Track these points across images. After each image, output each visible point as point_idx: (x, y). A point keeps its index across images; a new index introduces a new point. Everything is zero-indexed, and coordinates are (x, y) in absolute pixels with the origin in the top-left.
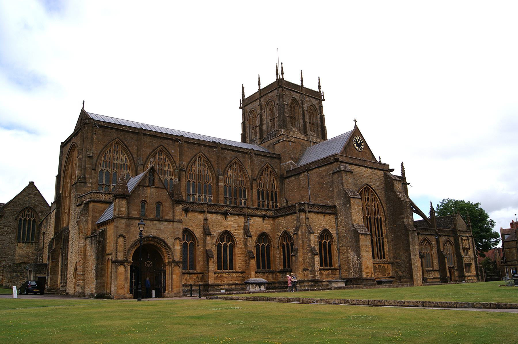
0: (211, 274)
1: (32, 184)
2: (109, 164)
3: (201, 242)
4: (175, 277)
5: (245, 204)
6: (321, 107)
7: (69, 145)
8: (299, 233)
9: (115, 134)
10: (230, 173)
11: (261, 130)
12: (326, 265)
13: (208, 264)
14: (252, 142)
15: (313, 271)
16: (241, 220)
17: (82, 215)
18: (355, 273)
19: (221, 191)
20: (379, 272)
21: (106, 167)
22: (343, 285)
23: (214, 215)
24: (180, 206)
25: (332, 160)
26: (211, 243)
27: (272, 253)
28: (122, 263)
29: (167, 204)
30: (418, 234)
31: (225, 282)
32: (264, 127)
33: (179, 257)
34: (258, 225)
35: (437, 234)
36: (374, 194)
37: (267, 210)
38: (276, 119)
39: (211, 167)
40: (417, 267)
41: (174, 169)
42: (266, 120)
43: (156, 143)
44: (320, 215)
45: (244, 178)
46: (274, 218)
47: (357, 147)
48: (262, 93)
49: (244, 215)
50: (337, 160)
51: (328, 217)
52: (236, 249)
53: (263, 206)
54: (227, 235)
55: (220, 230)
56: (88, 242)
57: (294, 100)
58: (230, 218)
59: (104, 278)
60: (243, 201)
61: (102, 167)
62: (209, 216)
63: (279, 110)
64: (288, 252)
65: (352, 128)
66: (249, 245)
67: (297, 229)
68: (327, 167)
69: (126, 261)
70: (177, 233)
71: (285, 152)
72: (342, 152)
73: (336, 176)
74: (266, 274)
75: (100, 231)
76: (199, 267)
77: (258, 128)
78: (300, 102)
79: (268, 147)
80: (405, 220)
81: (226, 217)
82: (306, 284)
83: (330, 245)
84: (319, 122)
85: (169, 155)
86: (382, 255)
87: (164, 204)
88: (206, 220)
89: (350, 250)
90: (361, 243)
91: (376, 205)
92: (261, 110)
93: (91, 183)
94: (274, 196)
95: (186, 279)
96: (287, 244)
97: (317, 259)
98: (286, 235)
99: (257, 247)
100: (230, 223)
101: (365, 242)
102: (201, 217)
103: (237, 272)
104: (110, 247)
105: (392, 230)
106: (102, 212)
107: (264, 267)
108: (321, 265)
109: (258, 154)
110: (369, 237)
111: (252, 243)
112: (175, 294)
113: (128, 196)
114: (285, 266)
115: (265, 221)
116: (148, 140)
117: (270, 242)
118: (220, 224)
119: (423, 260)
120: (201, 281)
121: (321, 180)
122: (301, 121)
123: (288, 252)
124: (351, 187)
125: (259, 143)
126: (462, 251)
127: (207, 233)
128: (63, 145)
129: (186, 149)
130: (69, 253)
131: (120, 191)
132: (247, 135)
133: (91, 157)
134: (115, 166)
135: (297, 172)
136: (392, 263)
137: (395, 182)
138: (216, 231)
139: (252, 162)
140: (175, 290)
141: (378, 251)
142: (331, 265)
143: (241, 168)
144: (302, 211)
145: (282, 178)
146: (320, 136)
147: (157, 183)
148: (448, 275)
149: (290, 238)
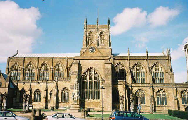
10: (57, 67)
20: (94, 105)
31: (36, 106)
43: (29, 61)
47: (91, 51)
55: (36, 89)
88: (31, 86)
91: (97, 76)
118: (35, 87)
138: (34, 90)
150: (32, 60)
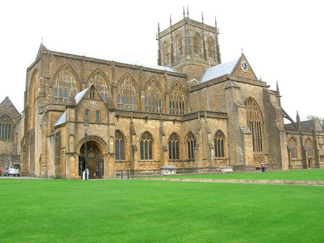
0: (136, 163)
1: (7, 98)
2: (62, 83)
3: (128, 139)
4: (110, 165)
5: (160, 111)
6: (217, 39)
7: (33, 70)
8: (200, 133)
9: (65, 61)
10: (149, 88)
11: (172, 56)
12: (219, 156)
13: (133, 155)
14: (165, 65)
15: (210, 161)
16: (158, 123)
17: (43, 120)
18: (240, 161)
19: (143, 102)
21: (60, 85)
22: (231, 170)
23: (138, 120)
24: (113, 113)
25: (225, 79)
26: (136, 140)
27: (180, 147)
28: (72, 154)
29: (104, 112)
30: (287, 134)
32: (175, 54)
33: (112, 150)
34: (170, 127)
35: (300, 134)
36: (256, 103)
37: (177, 116)
38: (184, 48)
39: (135, 85)
40: (285, 157)
41: (108, 86)
42: (176, 49)
43: (94, 67)
44: (215, 119)
45: (159, 92)
46: (181, 122)
48: (173, 28)
49: (160, 120)
50: (228, 79)
51: (221, 121)
52: (154, 144)
53: (174, 113)
54: (147, 134)
55: (143, 131)
56: (48, 139)
57: (197, 33)
58: (149, 122)
59: (60, 165)
60: (159, 109)
61: (57, 86)
62: (134, 120)
63: (186, 41)
64: (192, 147)
65: (239, 56)
66: (164, 141)
67: (199, 130)
68: (221, 84)
69: (75, 153)
70: (111, 133)
71: (190, 72)
72: (233, 73)
73: (227, 91)
74: (176, 163)
75: (56, 131)
76: (127, 158)
77: (170, 55)
78: (201, 35)
79: (178, 68)
80: (277, 124)
81: (146, 121)
82: (205, 170)
83: (222, 142)
84: (216, 50)
85: (104, 76)
86: (261, 149)
87: (101, 112)
88: (132, 123)
89: (237, 146)
90: (245, 140)
92: (172, 41)
93: (49, 97)
94: (182, 105)
95: (118, 166)
96: (192, 141)
97: (213, 152)
98: (190, 135)
99: (170, 143)
100: (149, 126)
101: (248, 140)
102: (128, 121)
103: (155, 161)
104: (64, 142)
105: (268, 130)
106: (58, 118)
107: (174, 158)
108: (216, 156)
109: (170, 74)
110: (251, 136)
111: (165, 140)
112: (111, 176)
113: (76, 106)
114: (189, 157)
115: (175, 124)
116: (89, 64)
117: (179, 139)
119: (290, 152)
120: (129, 168)
121: (217, 94)
122: (202, 49)
123: (192, 147)
124: (238, 99)
125: (170, 66)
126: (318, 146)
127: (132, 133)
128: (29, 70)
129: (116, 71)
130: (36, 148)
131: (69, 103)
132: (162, 60)
133: (49, 79)
134: (66, 84)
135: (199, 88)
136: (267, 155)
137: (271, 95)
138: (140, 132)
139: (166, 80)
140: (111, 174)
141: (258, 145)
142: (223, 156)
143: (158, 85)
144: (202, 116)
145: (188, 92)
146: (217, 60)
147: (96, 97)
148: (308, 163)
149: (193, 136)
150: (102, 65)
